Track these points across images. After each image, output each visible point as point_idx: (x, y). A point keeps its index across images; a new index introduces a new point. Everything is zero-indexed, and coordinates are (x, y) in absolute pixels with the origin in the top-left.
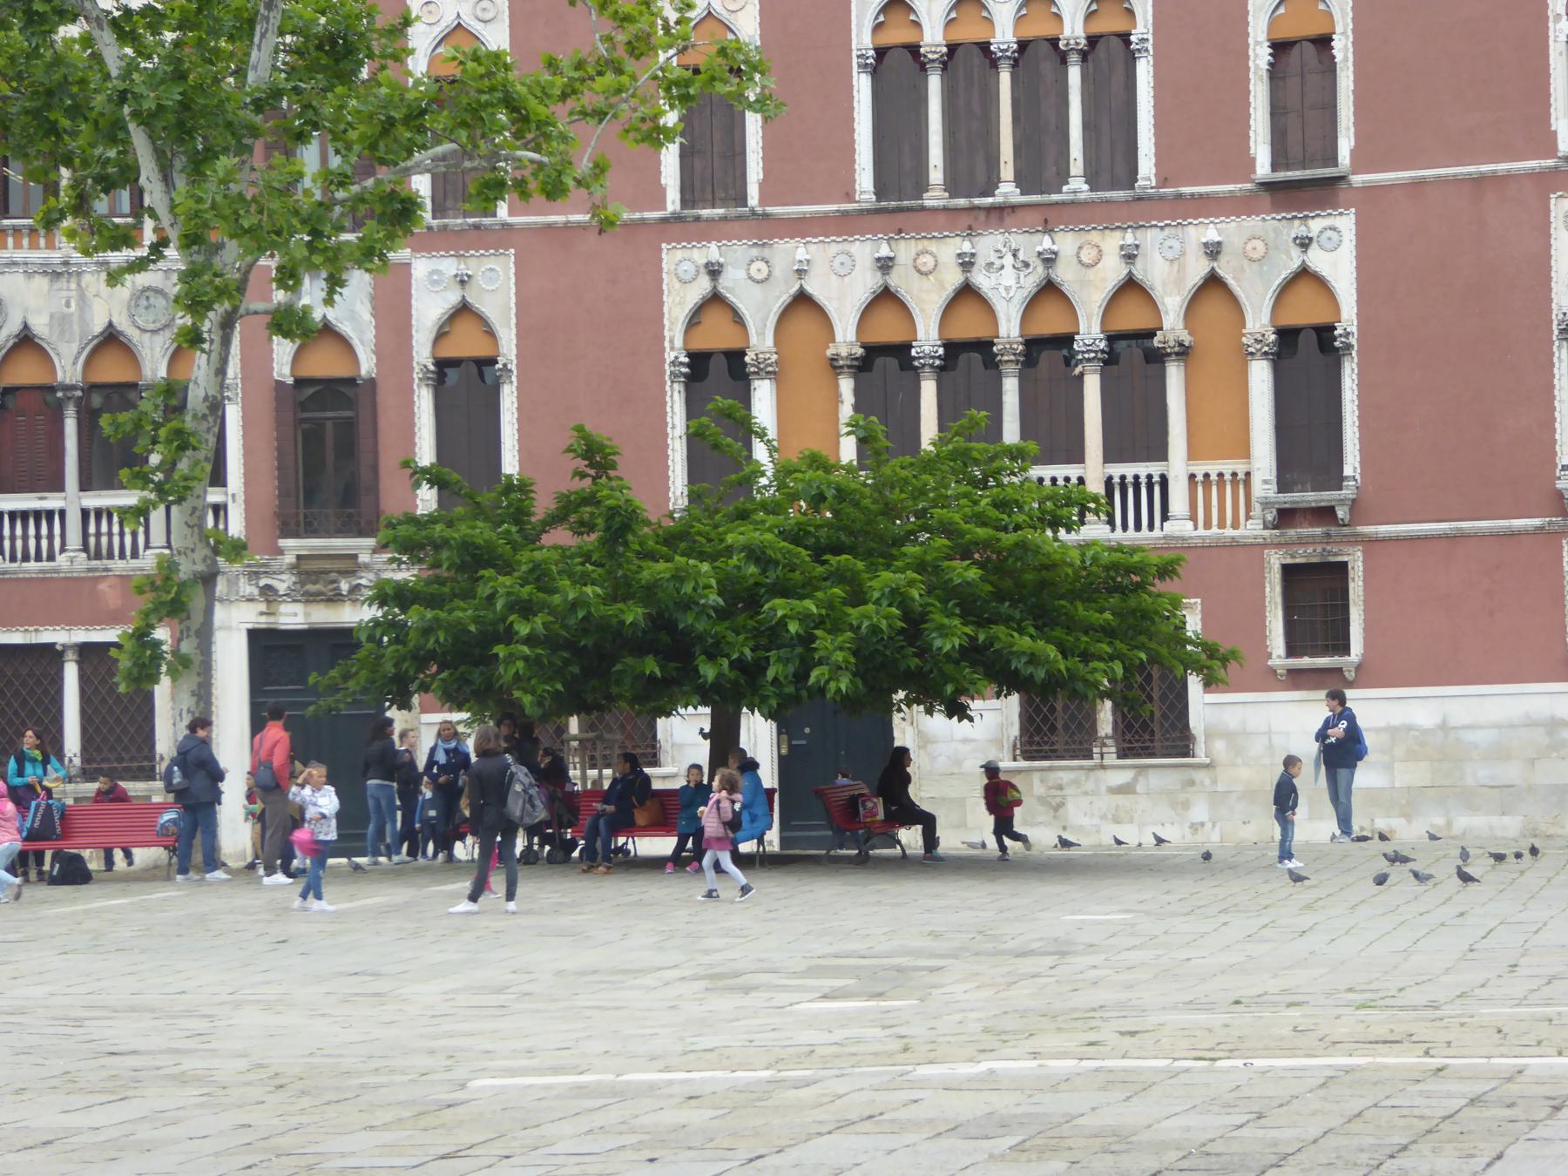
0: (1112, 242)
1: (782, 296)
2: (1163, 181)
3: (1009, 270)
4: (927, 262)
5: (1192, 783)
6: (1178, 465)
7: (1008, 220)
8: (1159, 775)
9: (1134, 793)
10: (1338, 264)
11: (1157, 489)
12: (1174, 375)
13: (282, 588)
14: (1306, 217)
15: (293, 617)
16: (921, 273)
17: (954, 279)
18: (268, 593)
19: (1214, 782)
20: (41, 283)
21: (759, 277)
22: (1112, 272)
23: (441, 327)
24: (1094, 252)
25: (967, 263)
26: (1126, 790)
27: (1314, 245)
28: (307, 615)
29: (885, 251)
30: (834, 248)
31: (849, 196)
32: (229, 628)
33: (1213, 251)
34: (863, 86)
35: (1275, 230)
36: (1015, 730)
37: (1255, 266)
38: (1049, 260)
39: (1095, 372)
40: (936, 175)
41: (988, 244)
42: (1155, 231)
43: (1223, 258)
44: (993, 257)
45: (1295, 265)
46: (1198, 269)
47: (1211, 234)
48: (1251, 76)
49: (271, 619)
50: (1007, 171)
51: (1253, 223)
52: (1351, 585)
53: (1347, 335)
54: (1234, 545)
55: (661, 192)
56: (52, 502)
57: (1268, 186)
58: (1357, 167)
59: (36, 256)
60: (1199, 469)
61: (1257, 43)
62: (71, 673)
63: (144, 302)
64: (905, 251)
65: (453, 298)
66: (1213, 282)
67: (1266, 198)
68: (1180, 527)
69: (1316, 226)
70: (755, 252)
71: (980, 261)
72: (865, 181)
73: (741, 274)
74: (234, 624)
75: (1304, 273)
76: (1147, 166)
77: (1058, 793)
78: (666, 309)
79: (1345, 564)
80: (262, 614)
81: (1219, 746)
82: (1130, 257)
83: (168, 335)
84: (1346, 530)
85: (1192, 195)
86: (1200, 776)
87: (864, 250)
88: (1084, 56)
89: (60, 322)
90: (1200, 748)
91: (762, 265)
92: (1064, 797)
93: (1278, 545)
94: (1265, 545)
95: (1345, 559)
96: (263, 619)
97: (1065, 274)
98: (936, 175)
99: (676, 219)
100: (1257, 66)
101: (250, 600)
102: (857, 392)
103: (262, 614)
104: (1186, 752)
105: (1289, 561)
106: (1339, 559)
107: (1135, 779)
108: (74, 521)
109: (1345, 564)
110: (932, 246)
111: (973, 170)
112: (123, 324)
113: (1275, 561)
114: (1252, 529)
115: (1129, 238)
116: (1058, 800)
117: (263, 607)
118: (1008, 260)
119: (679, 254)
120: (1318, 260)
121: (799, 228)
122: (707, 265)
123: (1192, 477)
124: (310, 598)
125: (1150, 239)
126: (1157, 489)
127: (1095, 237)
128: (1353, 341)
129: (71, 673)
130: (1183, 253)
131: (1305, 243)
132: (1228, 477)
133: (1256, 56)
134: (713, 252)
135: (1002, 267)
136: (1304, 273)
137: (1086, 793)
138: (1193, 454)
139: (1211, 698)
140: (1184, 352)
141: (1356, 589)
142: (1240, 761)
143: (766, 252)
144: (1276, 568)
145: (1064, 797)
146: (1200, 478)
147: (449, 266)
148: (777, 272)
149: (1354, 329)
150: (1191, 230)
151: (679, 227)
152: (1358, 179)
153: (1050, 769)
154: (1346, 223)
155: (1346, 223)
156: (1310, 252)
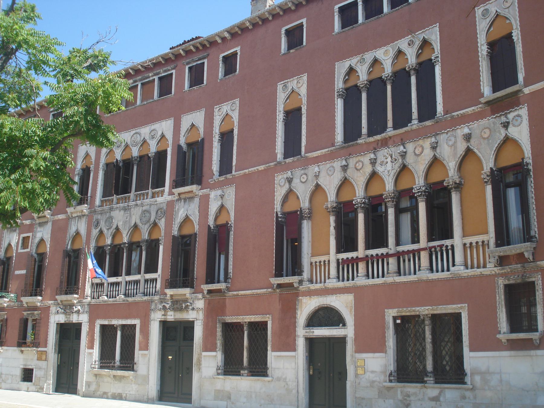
0: (427, 143)
1: (311, 187)
2: (446, 112)
3: (389, 163)
4: (359, 166)
5: (464, 397)
6: (457, 240)
7: (390, 142)
8: (451, 393)
9: (439, 400)
10: (521, 132)
11: (450, 252)
12: (455, 198)
13: (168, 306)
14: (506, 113)
15: (171, 316)
16: (357, 169)
17: (368, 169)
18: (164, 308)
19: (475, 398)
20: (122, 212)
21: (304, 180)
22: (428, 155)
23: (217, 214)
24: (420, 149)
25: (373, 162)
26: (436, 399)
27: (511, 126)
28: (174, 315)
29: (344, 163)
30: (328, 165)
31: (333, 145)
32: (154, 320)
33: (468, 138)
34: (339, 104)
35: (494, 123)
36: (392, 367)
37: (486, 141)
38: (404, 155)
39: (422, 201)
40: (364, 131)
41: (383, 154)
42: (445, 135)
43: (472, 141)
44: (383, 159)
45: (502, 137)
46: (462, 147)
47: (466, 131)
48: (480, 59)
49: (165, 317)
50: (390, 124)
51: (484, 122)
52: (537, 293)
53: (527, 164)
54: (481, 276)
55: (276, 155)
56: (119, 279)
57: (488, 103)
58: (526, 85)
59: (121, 205)
60: (468, 240)
61: (482, 45)
62: (119, 333)
63: (144, 215)
64: (352, 162)
65: (220, 203)
66: (469, 151)
67: (488, 108)
68: (459, 269)
69: (511, 116)
70: (303, 172)
71: (379, 161)
72: (339, 137)
73: (299, 180)
74: (156, 319)
75: (507, 140)
76: (440, 108)
77: (408, 399)
78: (275, 198)
79: (533, 283)
80: (163, 315)
81: (477, 378)
82: (434, 148)
83: (148, 224)
84: (532, 264)
85: (458, 115)
86: (468, 394)
87: (338, 164)
88: (417, 71)
89: (125, 223)
90: (468, 379)
91: (304, 176)
92: (410, 401)
93: (502, 275)
94: (496, 275)
95: (533, 279)
96: (163, 317)
97: (410, 160)
98: (364, 131)
99: (280, 163)
100: (482, 54)
101: (160, 310)
102: (336, 221)
103: (163, 315)
104: (465, 383)
105: (507, 282)
106: (531, 280)
107: (440, 394)
108: (124, 284)
109: (533, 283)
110: (361, 159)
111: (377, 126)
112: (138, 222)
113: (501, 282)
114: (491, 269)
115: (433, 140)
116: (408, 402)
117: (163, 313)
118: (389, 159)
119: (280, 177)
120: (513, 132)
121: (317, 160)
122: (287, 178)
123: (465, 245)
124: (175, 310)
125: (442, 138)
126: (450, 252)
127: (421, 142)
128: (531, 167)
129: (119, 333)
130: (455, 142)
131: (506, 125)
132: (480, 243)
133: (482, 50)
134: (289, 174)
135: (387, 162)
136: (507, 140)
137: (419, 400)
138: (465, 235)
139: (472, 354)
140: (458, 186)
141: (539, 294)
142: (487, 388)
143: (306, 171)
144: (502, 286)
145: (410, 401)
146: (468, 245)
147: (219, 192)
148: (310, 178)
149: (531, 161)
150: (459, 131)
151: (280, 167)
152: (527, 91)
153: (404, 387)
154: (523, 111)
155: (523, 111)
156: (509, 129)
